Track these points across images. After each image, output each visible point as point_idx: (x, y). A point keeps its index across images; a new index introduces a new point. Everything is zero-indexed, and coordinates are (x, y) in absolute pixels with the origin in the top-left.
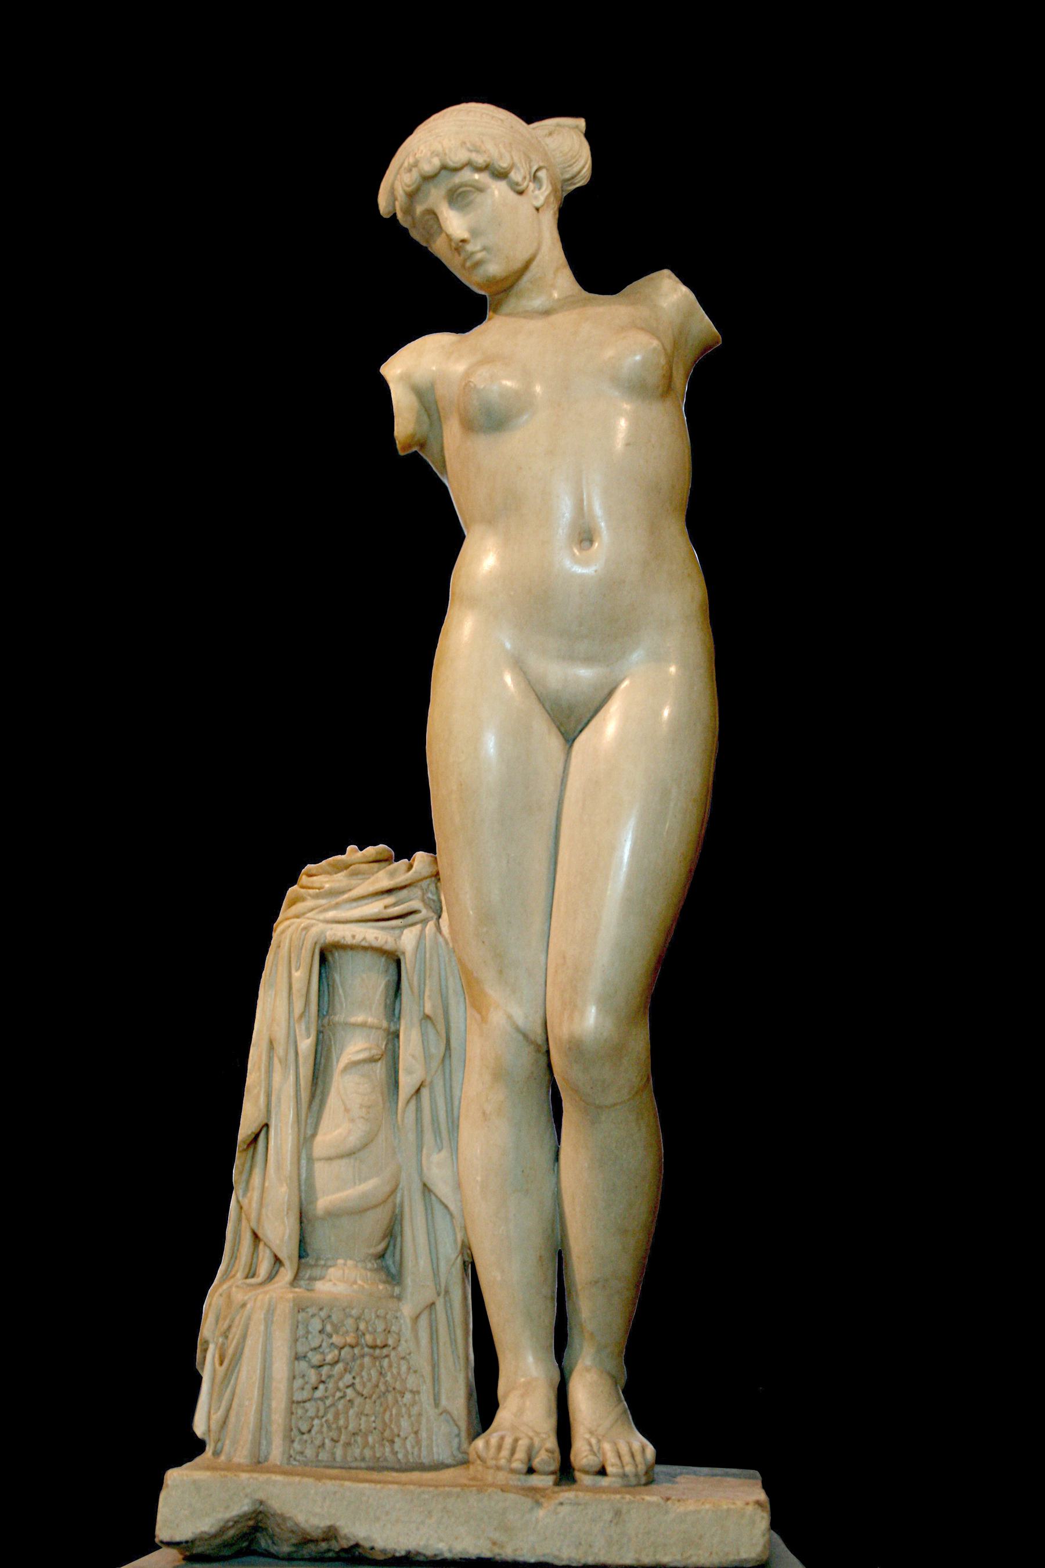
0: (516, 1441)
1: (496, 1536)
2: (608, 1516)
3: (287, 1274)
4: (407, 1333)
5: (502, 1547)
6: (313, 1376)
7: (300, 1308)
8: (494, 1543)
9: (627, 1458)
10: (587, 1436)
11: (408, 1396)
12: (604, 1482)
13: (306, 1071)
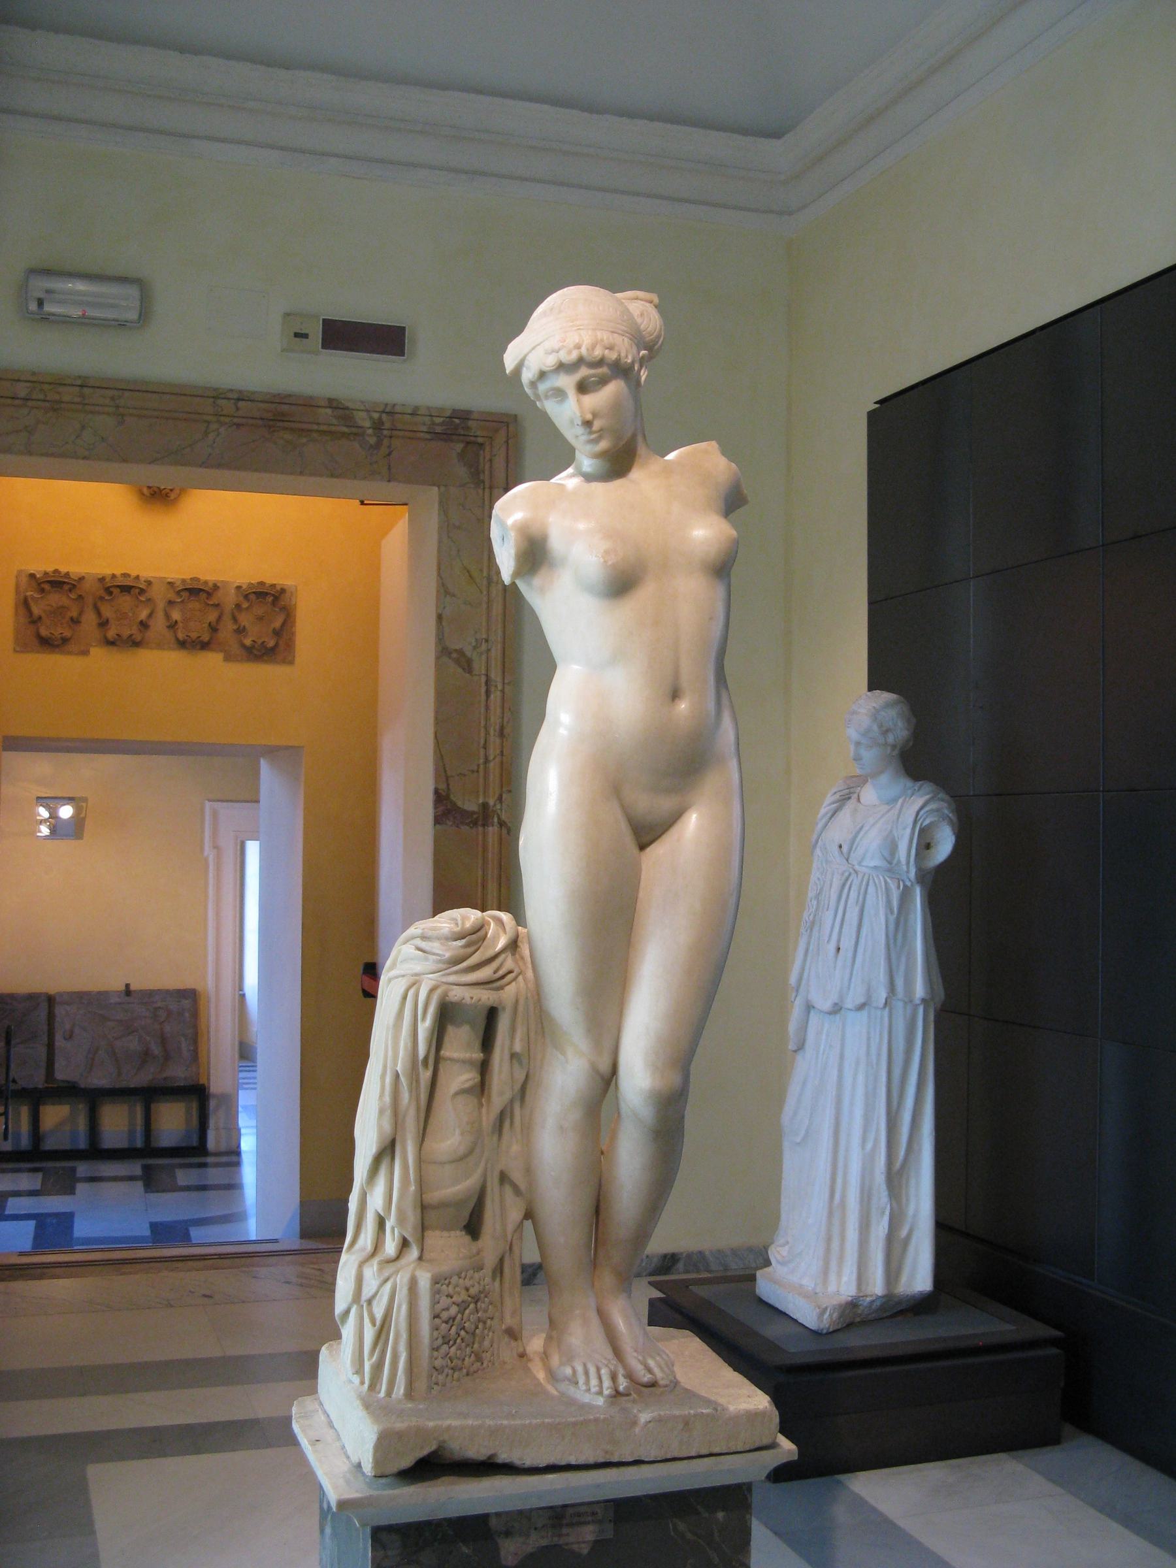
0: (598, 1370)
1: (609, 1447)
2: (681, 1426)
3: (414, 1253)
4: (488, 1280)
7: (436, 1281)
8: (607, 1452)
11: (489, 1321)
13: (424, 1097)
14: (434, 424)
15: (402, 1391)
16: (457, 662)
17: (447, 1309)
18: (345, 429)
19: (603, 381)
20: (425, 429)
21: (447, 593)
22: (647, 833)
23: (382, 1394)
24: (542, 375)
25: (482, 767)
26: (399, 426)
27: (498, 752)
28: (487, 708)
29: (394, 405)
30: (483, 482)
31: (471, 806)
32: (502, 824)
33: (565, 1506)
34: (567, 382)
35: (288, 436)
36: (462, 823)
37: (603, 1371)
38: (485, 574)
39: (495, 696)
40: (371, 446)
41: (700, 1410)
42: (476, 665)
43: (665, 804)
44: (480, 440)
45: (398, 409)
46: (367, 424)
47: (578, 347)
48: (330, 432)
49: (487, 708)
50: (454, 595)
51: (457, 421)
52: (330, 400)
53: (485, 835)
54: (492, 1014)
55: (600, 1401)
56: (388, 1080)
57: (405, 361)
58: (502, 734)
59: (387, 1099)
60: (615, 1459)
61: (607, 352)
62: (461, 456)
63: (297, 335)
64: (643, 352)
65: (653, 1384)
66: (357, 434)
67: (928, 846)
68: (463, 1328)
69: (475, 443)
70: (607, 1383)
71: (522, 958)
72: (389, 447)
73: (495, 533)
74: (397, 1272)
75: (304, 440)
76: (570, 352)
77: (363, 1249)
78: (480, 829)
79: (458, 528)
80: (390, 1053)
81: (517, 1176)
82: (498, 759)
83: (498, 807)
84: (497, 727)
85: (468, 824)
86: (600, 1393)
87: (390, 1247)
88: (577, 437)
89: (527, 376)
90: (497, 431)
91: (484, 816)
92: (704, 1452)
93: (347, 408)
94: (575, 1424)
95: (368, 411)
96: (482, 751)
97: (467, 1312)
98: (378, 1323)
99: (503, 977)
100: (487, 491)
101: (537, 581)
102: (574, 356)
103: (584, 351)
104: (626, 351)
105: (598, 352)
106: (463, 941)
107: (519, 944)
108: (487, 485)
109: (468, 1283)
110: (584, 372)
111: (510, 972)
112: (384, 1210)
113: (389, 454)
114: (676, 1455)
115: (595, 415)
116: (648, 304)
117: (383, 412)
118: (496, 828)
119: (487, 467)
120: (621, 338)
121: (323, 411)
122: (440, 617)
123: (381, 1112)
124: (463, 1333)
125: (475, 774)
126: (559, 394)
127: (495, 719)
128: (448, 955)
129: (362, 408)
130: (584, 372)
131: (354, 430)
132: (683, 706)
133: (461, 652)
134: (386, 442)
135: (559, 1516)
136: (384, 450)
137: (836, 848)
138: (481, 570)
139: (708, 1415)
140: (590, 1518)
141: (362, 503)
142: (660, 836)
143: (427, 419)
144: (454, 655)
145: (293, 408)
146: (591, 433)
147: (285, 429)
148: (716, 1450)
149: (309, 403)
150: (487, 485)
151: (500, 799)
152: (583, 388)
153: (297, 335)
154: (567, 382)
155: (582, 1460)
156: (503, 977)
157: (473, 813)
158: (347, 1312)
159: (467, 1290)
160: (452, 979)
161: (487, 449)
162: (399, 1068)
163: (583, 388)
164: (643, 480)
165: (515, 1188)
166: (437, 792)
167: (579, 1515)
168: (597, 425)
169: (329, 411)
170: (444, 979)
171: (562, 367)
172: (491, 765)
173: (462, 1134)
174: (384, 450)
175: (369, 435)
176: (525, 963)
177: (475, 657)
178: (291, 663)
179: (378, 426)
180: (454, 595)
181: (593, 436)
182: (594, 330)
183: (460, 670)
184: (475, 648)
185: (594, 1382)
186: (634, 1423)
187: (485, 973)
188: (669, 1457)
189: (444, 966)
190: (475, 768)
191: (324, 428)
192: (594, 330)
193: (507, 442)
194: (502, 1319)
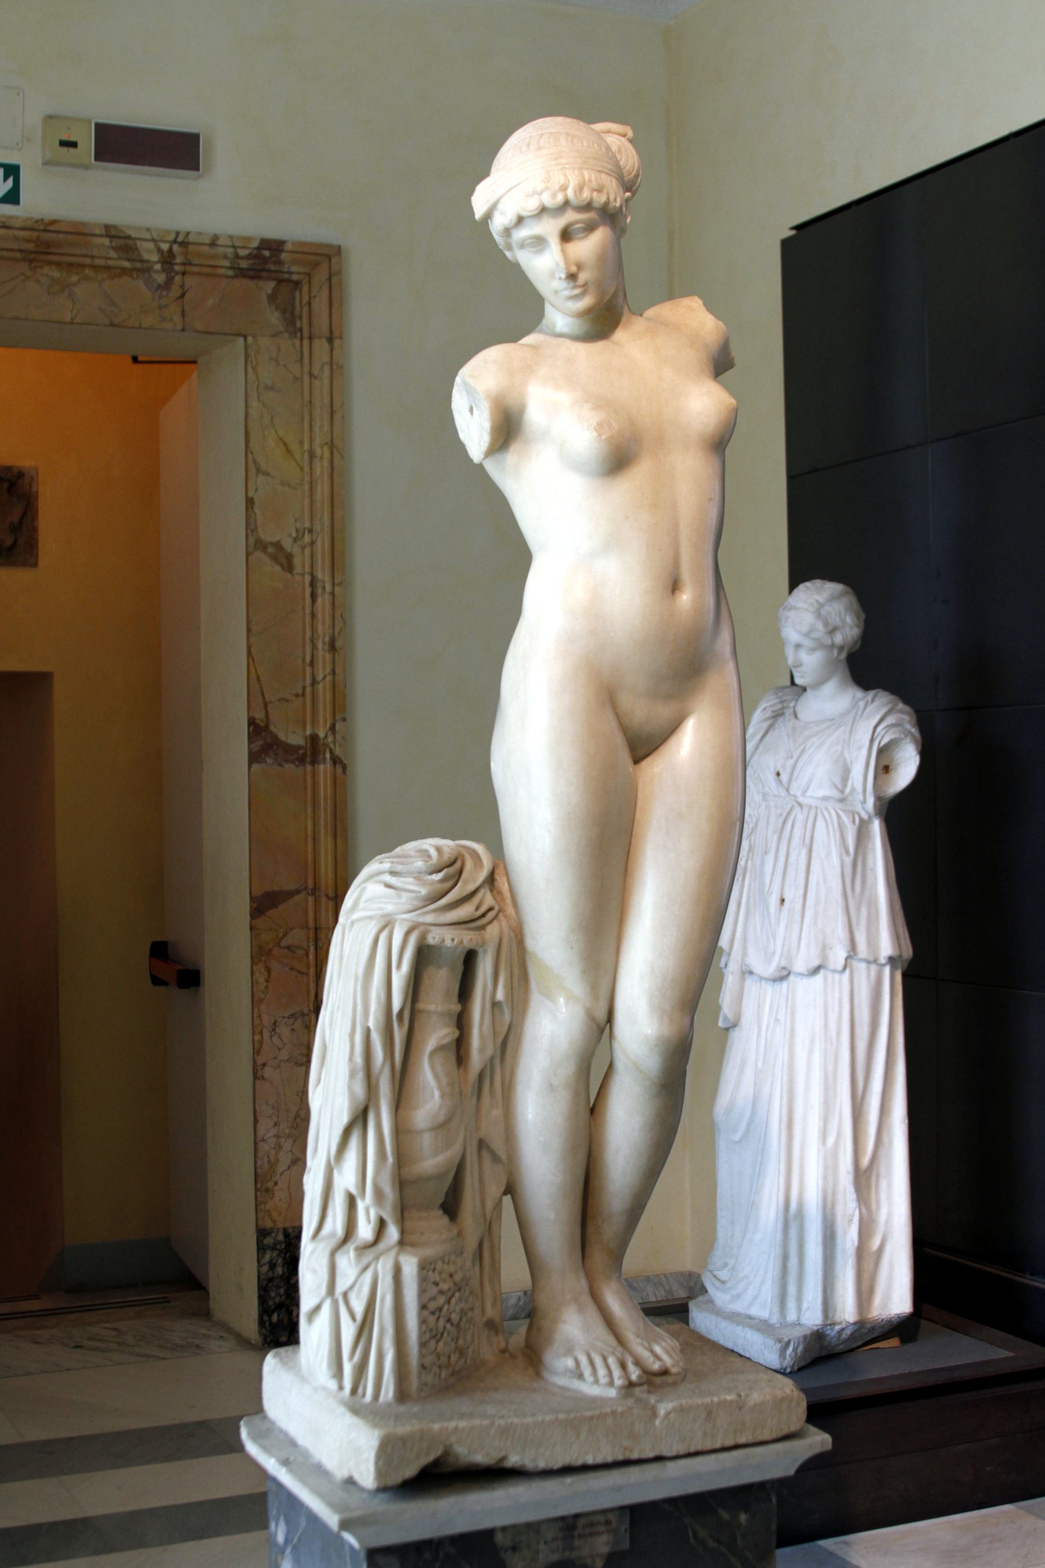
1: (627, 1443)
2: (704, 1416)
3: (393, 1233)
4: (469, 1264)
5: (631, 1451)
6: (432, 1319)
7: (424, 1267)
8: (625, 1449)
9: (674, 1356)
10: (639, 1340)
12: (669, 1379)
14: (237, 256)
15: (391, 1394)
16: (274, 558)
17: (433, 1299)
18: (126, 264)
19: (590, 228)
20: (227, 263)
21: (258, 471)
22: (644, 745)
23: (369, 1397)
24: (520, 220)
25: (308, 690)
26: (195, 261)
27: (328, 670)
28: (313, 615)
29: (188, 234)
30: (301, 330)
31: (296, 739)
32: (336, 761)
33: (576, 1516)
35: (56, 274)
36: (286, 761)
37: (611, 1360)
38: (306, 447)
39: (323, 602)
40: (159, 286)
41: (722, 1397)
42: (297, 562)
43: (664, 712)
44: (295, 277)
45: (191, 238)
46: (155, 257)
47: (564, 188)
48: (108, 268)
49: (313, 615)
50: (268, 474)
51: (267, 253)
52: (107, 227)
53: (315, 775)
54: (470, 958)
55: (612, 1393)
56: (358, 1038)
57: (198, 177)
58: (332, 648)
59: (359, 1059)
60: (635, 1456)
61: (595, 194)
62: (272, 298)
63: (64, 144)
64: (628, 194)
65: (665, 1372)
66: (144, 269)
67: (887, 769)
68: (449, 1320)
69: (289, 281)
70: (617, 1372)
71: (500, 893)
72: (182, 286)
73: (459, 402)
74: (377, 1258)
75: (75, 279)
76: (554, 195)
77: (333, 1234)
78: (309, 768)
79: (272, 388)
80: (359, 1007)
81: (498, 1144)
82: (329, 678)
83: (330, 739)
84: (327, 639)
85: (292, 762)
86: (611, 1383)
87: (365, 1231)
88: (556, 292)
89: (498, 224)
90: (316, 265)
91: (312, 752)
92: (729, 1443)
93: (129, 237)
94: (591, 1418)
95: (154, 240)
96: (308, 670)
97: (453, 1301)
98: (359, 1317)
99: (483, 915)
100: (306, 342)
101: (511, 457)
102: (560, 198)
103: (570, 193)
104: (613, 195)
105: (586, 194)
106: (440, 876)
107: (496, 876)
108: (306, 334)
109: (452, 1269)
110: (570, 216)
111: (491, 909)
112: (357, 1187)
113: (183, 295)
114: (700, 1448)
115: (580, 267)
116: (623, 139)
117: (175, 241)
118: (329, 765)
119: (305, 309)
120: (610, 178)
121: (99, 240)
122: (250, 502)
123: (352, 1075)
124: (448, 1326)
125: (301, 699)
126: (539, 242)
127: (323, 630)
128: (424, 891)
129: (148, 236)
130: (570, 216)
131: (138, 265)
132: (685, 598)
133: (278, 546)
134: (178, 279)
135: (570, 1526)
136: (175, 291)
137: (774, 774)
138: (301, 443)
139: (731, 1402)
140: (602, 1528)
141: (135, 360)
142: (656, 749)
143: (230, 251)
144: (270, 550)
145: (61, 236)
146: (575, 287)
147: (50, 263)
148: (742, 1440)
149: (79, 232)
150: (306, 334)
151: (333, 728)
153: (64, 144)
154: (550, 228)
155: (599, 1459)
156: (483, 915)
157: (299, 747)
158: (317, 1308)
159: (451, 1276)
160: (429, 919)
161: (305, 288)
162: (371, 1024)
163: (566, 236)
164: (630, 341)
165: (496, 1158)
166: (251, 722)
167: (592, 1525)
168: (583, 277)
169: (106, 241)
170: (421, 920)
171: (543, 210)
172: (320, 686)
173: (442, 1096)
174: (175, 291)
175: (157, 272)
176: (503, 899)
177: (296, 550)
178: (35, 565)
179: (167, 259)
180: (268, 474)
182: (581, 168)
183: (278, 568)
184: (295, 540)
185: (602, 1372)
186: (654, 1415)
187: (465, 911)
188: (692, 1450)
189: (421, 904)
190: (300, 692)
191: (102, 262)
192: (581, 168)
193: (330, 280)
194: (483, 1311)
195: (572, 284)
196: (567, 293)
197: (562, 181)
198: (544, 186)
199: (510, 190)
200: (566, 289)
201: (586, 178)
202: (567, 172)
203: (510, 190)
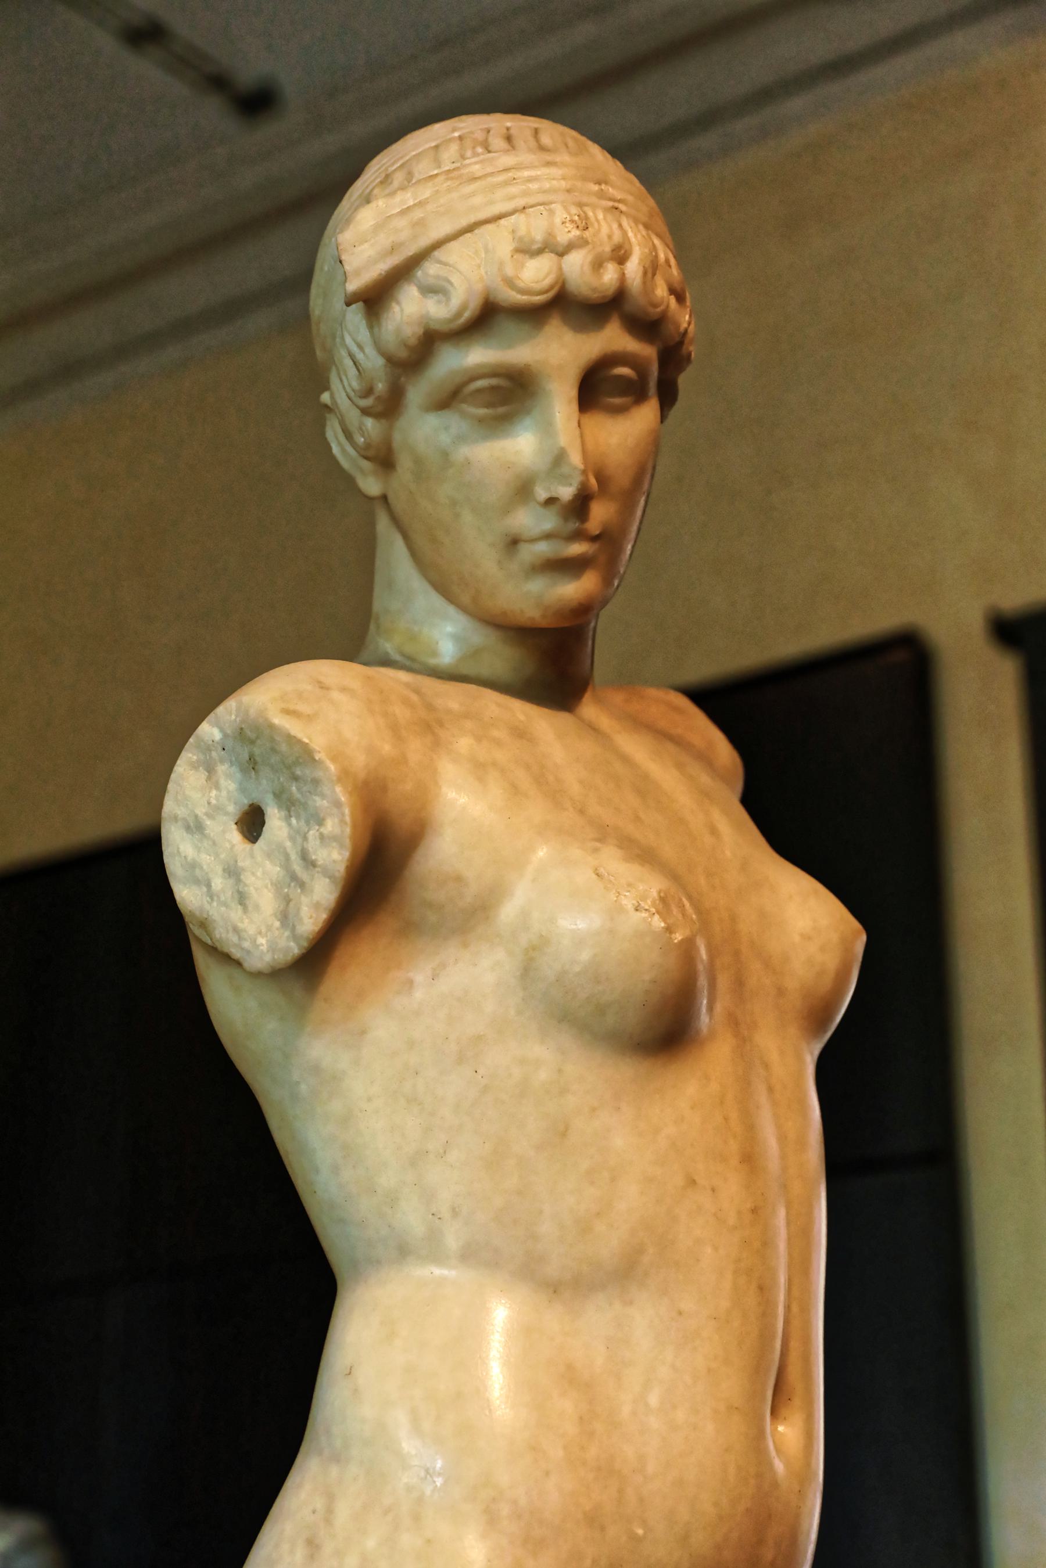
19: (635, 391)
24: (487, 317)
34: (559, 354)
76: (598, 265)
88: (514, 542)
126: (511, 394)
130: (613, 338)
146: (578, 535)
152: (595, 389)
154: (559, 354)
163: (595, 389)
168: (600, 513)
171: (563, 305)
181: (577, 549)
195: (573, 525)
196: (543, 549)
197: (617, 237)
198: (576, 233)
199: (470, 229)
200: (548, 536)
201: (662, 256)
202: (625, 222)
203: (470, 229)
